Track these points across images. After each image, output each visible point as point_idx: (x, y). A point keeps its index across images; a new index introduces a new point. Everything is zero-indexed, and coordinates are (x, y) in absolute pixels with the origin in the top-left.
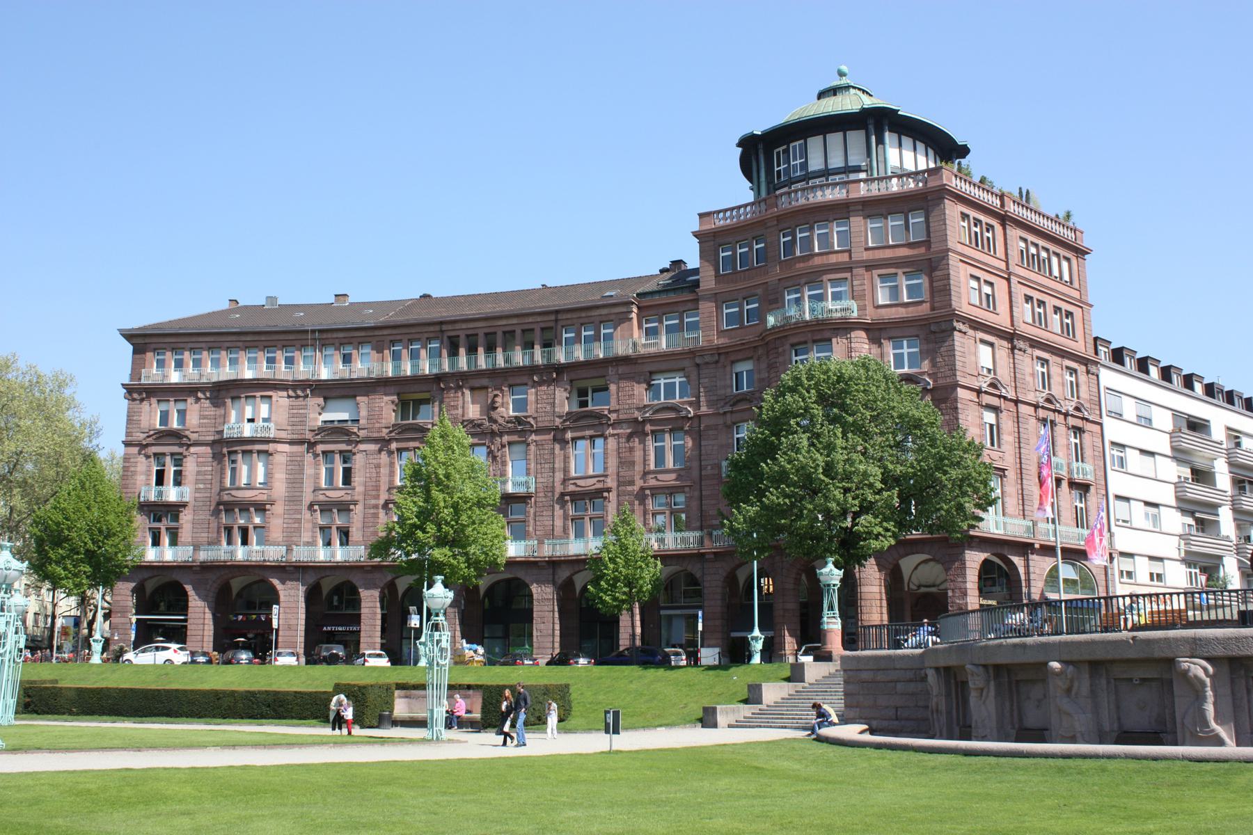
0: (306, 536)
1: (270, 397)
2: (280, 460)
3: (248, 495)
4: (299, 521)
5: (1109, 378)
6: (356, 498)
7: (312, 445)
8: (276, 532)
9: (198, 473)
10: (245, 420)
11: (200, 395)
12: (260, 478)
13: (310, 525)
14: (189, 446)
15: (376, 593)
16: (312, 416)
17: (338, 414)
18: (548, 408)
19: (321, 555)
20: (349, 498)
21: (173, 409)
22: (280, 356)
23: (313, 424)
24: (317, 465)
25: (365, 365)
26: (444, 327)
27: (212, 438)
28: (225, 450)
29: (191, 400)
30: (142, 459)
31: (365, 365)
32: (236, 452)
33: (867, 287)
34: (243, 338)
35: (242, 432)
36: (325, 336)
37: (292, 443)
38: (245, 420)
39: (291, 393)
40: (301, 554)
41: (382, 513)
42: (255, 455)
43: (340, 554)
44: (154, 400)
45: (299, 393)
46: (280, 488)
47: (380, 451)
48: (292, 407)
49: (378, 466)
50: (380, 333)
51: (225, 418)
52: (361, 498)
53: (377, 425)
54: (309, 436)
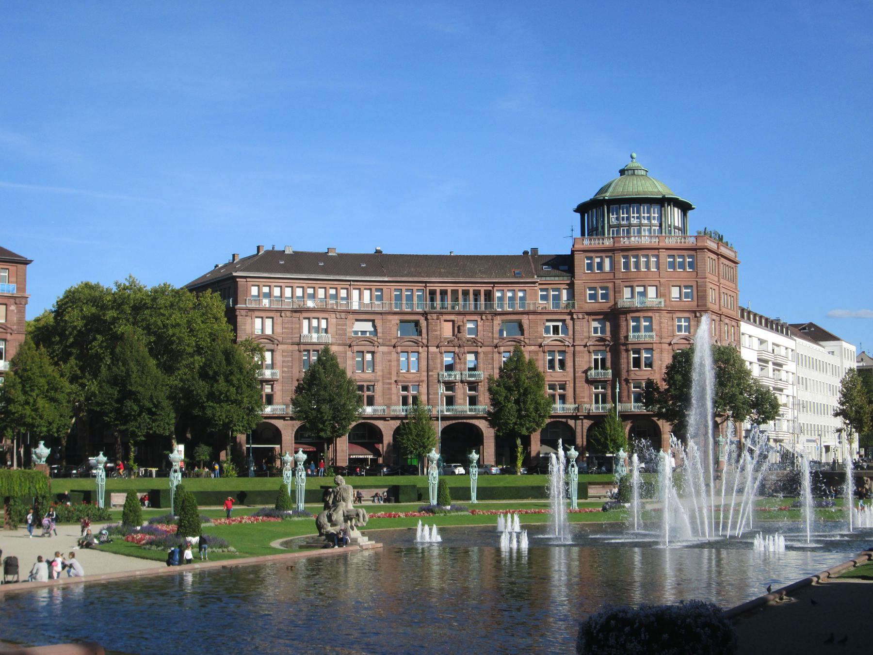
5: (745, 327)
9: (283, 361)
18: (490, 334)
33: (667, 291)
39: (338, 316)
41: (394, 386)
48: (337, 325)
49: (390, 361)
52: (381, 378)
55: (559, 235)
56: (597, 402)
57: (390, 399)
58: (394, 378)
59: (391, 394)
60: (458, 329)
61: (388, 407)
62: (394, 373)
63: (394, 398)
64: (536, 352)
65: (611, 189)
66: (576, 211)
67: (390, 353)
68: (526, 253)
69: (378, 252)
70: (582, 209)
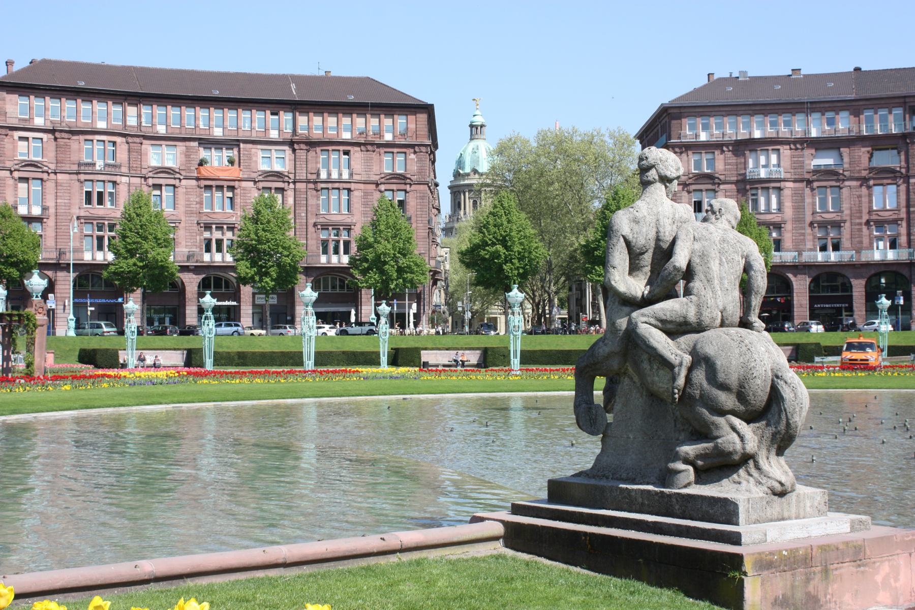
0: (809, 245)
1: (779, 150)
2: (787, 193)
3: (768, 217)
4: (803, 234)
6: (844, 218)
7: (809, 182)
8: (787, 242)
10: (762, 166)
11: (725, 149)
12: (774, 205)
13: (811, 237)
14: (719, 184)
15: (863, 282)
16: (807, 162)
17: (826, 161)
19: (820, 257)
20: (839, 218)
21: (705, 157)
22: (781, 119)
23: (808, 167)
24: (813, 196)
25: (844, 125)
26: (907, 100)
27: (735, 179)
28: (748, 187)
29: (717, 152)
30: (685, 194)
31: (844, 125)
32: (757, 188)
34: (754, 108)
35: (759, 175)
36: (814, 106)
37: (795, 181)
38: (762, 166)
39: (792, 146)
40: (807, 257)
41: (864, 228)
42: (760, 191)
43: (833, 257)
44: (690, 153)
45: (798, 146)
46: (789, 211)
47: (861, 186)
48: (792, 156)
49: (860, 196)
50: (857, 103)
51: (745, 163)
52: (848, 218)
53: (858, 168)
54: (807, 176)
57: (861, 242)
58: (865, 217)
59: (861, 236)
61: (858, 251)
62: (865, 210)
63: (866, 241)
69: (857, 69)
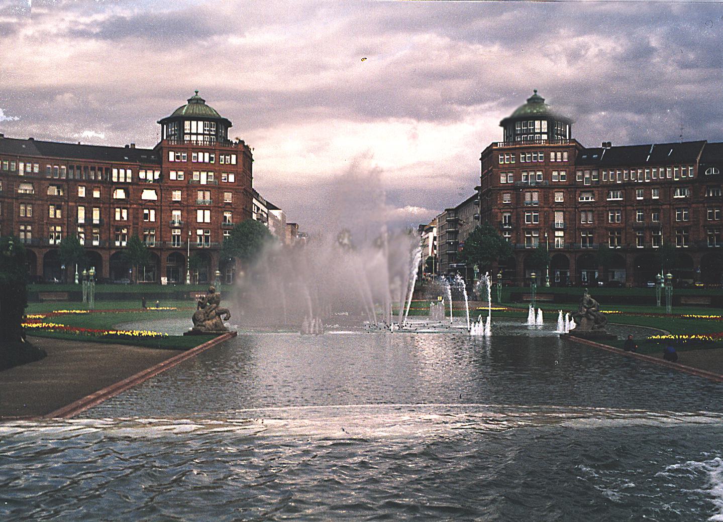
18: (108, 196)
49: (43, 210)
55: (148, 138)
56: (174, 241)
60: (89, 192)
64: (137, 209)
65: (184, 111)
66: (158, 122)
67: (43, 205)
68: (127, 146)
70: (162, 122)
